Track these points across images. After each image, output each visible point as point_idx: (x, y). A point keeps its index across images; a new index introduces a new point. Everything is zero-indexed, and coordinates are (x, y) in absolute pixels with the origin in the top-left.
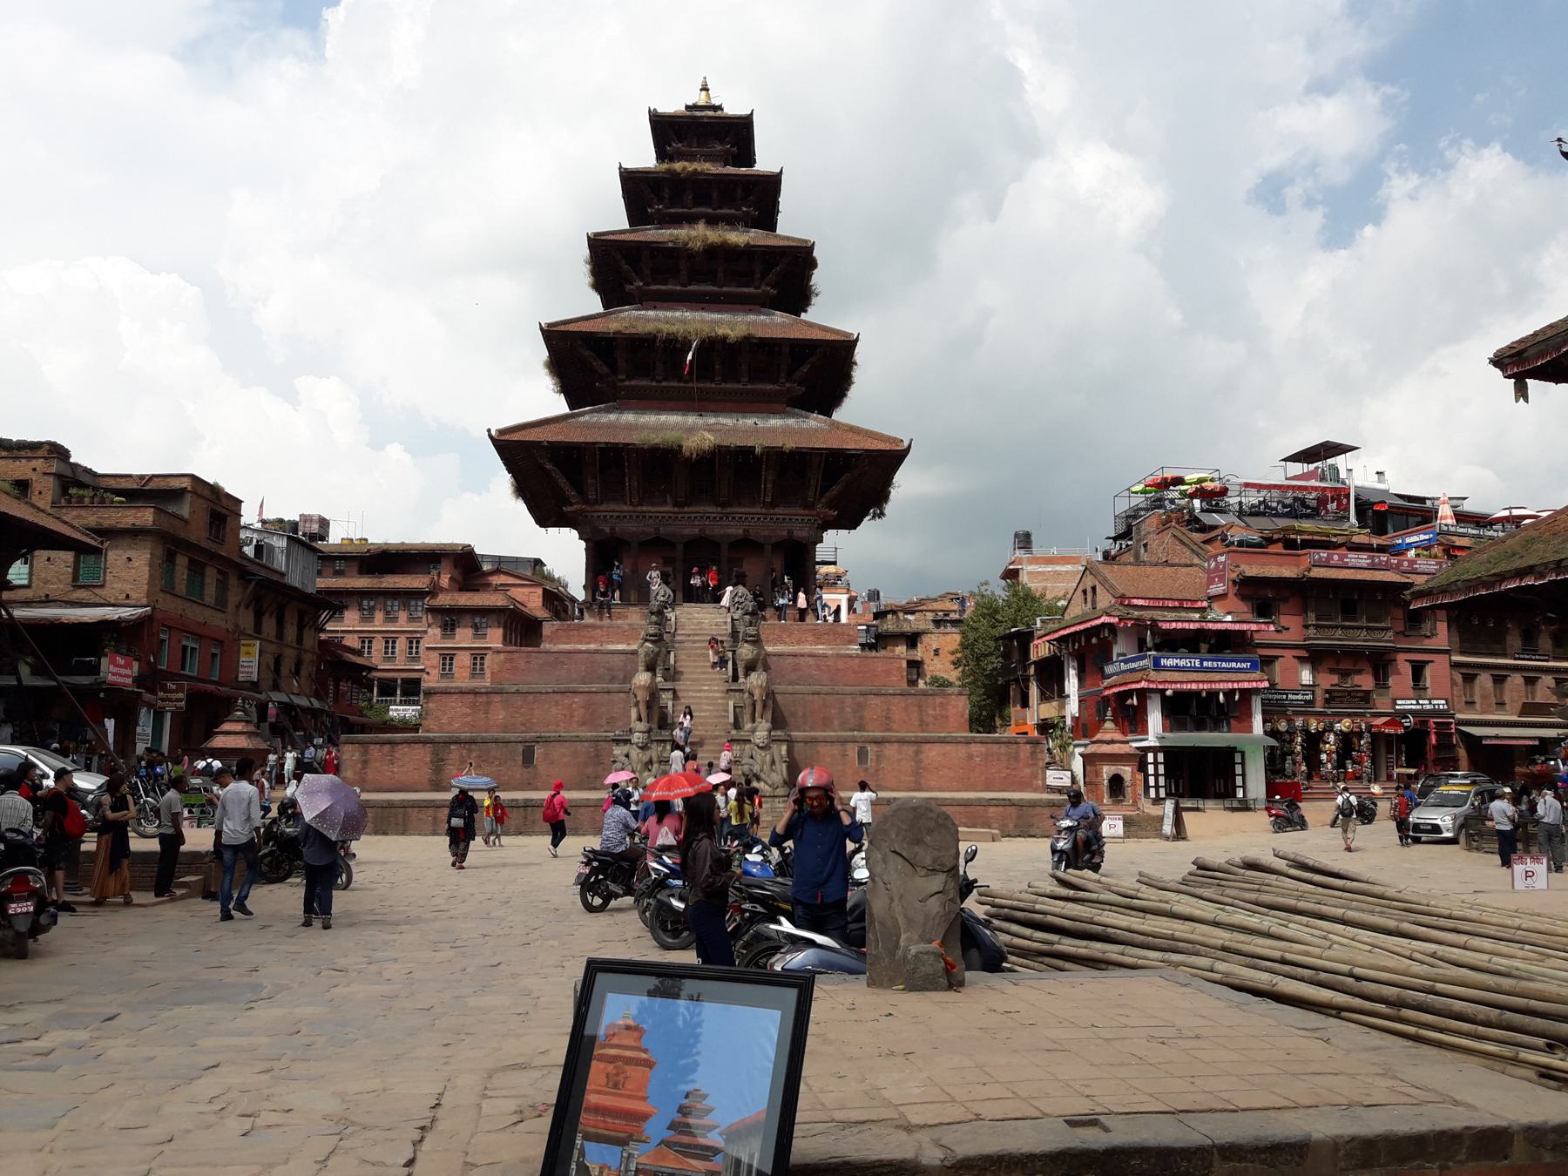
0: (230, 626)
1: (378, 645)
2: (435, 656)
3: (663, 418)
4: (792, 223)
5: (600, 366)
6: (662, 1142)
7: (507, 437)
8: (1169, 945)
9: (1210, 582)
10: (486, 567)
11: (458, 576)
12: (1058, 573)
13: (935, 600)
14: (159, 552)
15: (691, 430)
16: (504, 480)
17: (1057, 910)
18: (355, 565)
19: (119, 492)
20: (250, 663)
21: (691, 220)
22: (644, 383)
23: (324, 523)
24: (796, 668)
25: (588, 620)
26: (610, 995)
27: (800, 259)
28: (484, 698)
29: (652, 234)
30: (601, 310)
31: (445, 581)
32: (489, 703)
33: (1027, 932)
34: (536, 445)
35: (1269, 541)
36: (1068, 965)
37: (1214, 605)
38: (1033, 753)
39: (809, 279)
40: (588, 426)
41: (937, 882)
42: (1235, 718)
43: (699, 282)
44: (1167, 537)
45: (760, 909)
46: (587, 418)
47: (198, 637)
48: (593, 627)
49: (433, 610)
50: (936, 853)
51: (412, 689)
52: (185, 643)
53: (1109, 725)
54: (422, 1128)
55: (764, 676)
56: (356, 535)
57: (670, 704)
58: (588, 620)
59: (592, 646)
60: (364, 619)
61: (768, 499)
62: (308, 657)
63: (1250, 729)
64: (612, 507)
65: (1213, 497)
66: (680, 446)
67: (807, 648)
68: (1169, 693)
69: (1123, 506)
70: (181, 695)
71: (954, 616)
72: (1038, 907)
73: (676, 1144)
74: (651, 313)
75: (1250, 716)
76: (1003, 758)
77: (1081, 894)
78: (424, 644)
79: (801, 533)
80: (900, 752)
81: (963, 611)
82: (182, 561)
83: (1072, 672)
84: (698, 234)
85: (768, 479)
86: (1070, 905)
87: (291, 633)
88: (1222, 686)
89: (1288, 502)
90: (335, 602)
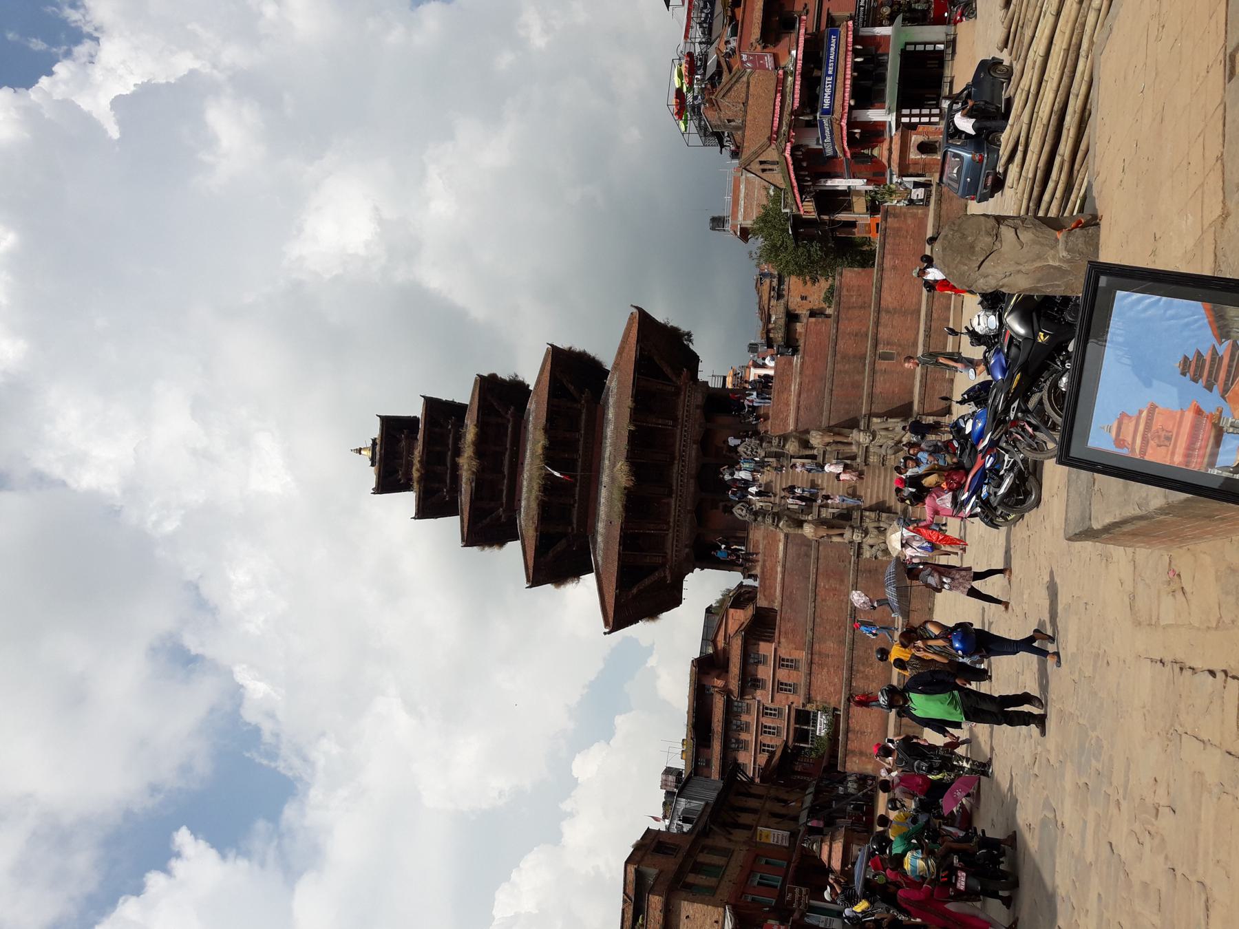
0: (745, 848)
1: (767, 739)
2: (778, 696)
3: (603, 500)
4: (461, 392)
5: (561, 545)
6: (1223, 397)
7: (611, 620)
8: (1074, 51)
9: (763, 67)
10: (710, 651)
12: (747, 195)
13: (761, 298)
14: (684, 894)
15: (613, 479)
17: (1035, 157)
19: (635, 919)
20: (775, 836)
21: (456, 467)
23: (668, 771)
25: (757, 571)
26: (1089, 445)
27: (489, 387)
28: (816, 658)
29: (465, 498)
30: (519, 542)
31: (719, 683)
32: (820, 654)
33: (1051, 185)
35: (733, 18)
36: (1083, 147)
37: (783, 64)
38: (895, 216)
39: (503, 381)
40: (606, 558)
41: (1007, 233)
42: (877, 49)
43: (502, 464)
44: (724, 102)
45: (1015, 405)
46: (599, 559)
47: (752, 872)
49: (742, 693)
50: (983, 233)
51: (804, 717)
52: (755, 883)
53: (876, 152)
54: (1181, 669)
55: (813, 433)
56: (679, 748)
57: (831, 510)
58: (757, 571)
59: (779, 569)
60: (746, 748)
61: (671, 423)
62: (773, 792)
63: (887, 38)
64: (669, 544)
65: (693, 64)
66: (625, 488)
67: (793, 398)
68: (852, 103)
69: (696, 139)
70: (797, 890)
71: (775, 283)
72: (1030, 175)
73: (1226, 384)
74: (523, 503)
75: (874, 37)
77: (1022, 140)
78: (768, 704)
79: (699, 399)
80: (886, 326)
81: (771, 275)
82: (691, 878)
83: (830, 183)
84: (467, 463)
86: (1031, 147)
87: (753, 803)
88: (849, 60)
89: (702, 5)
90: (731, 768)
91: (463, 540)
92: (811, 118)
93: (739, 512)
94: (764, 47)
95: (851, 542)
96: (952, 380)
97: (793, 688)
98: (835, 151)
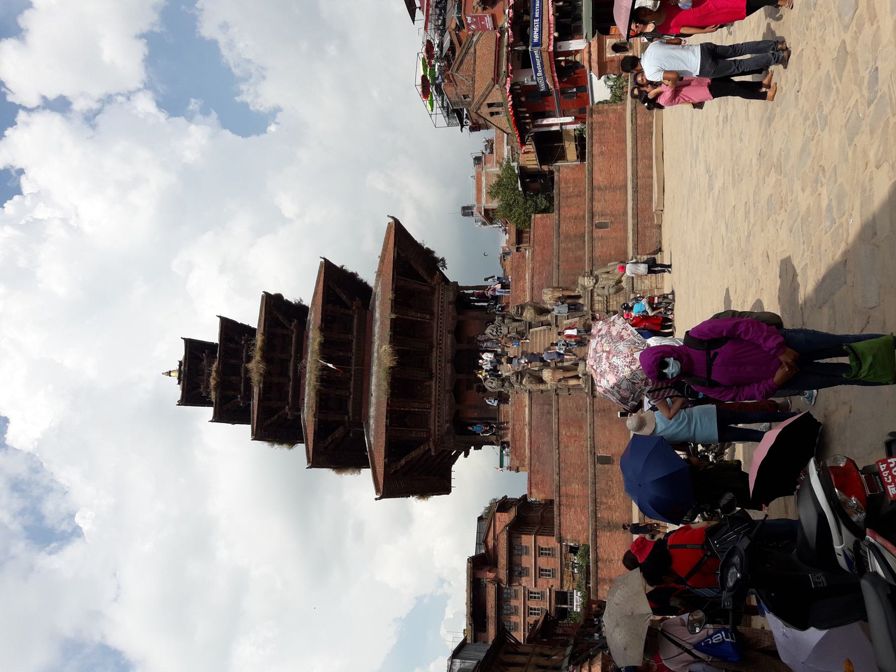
3: (373, 388)
5: (339, 433)
7: (381, 487)
9: (484, 28)
10: (483, 551)
11: (488, 568)
15: (380, 365)
16: (412, 500)
18: (479, 634)
22: (350, 404)
25: (508, 438)
28: (564, 500)
31: (491, 575)
32: (567, 495)
34: (387, 466)
38: (599, 113)
39: (288, 303)
44: (459, 76)
46: (372, 439)
48: (514, 429)
49: (510, 581)
51: (563, 597)
58: (508, 438)
59: (527, 431)
61: (428, 317)
62: (538, 650)
66: (391, 368)
67: (528, 285)
68: (556, 34)
76: (602, 132)
79: (451, 296)
80: (599, 201)
83: (546, 122)
85: (414, 315)
89: (438, 12)
91: (253, 434)
92: (524, 48)
94: (484, 9)
96: (660, 226)
97: (550, 573)
98: (547, 85)
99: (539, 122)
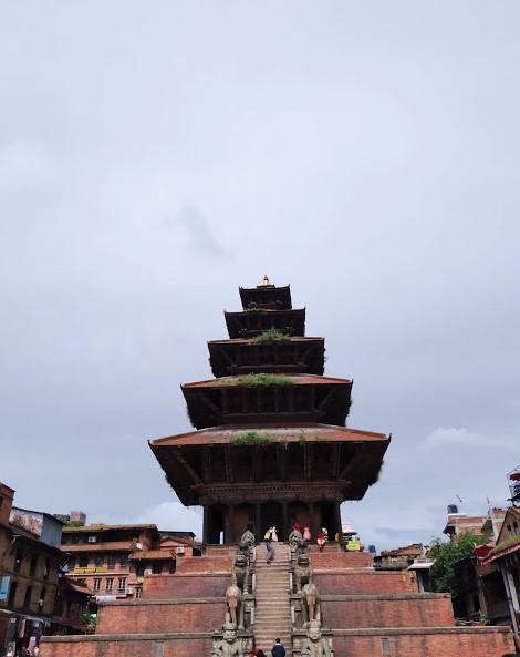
5: (213, 407)
11: (147, 540)
24: (334, 583)
27: (317, 347)
28: (134, 609)
29: (240, 341)
32: (138, 612)
38: (505, 640)
43: (267, 363)
48: (208, 560)
49: (133, 561)
55: (314, 587)
61: (309, 475)
62: (51, 588)
67: (341, 570)
76: (484, 644)
78: (127, 582)
83: (511, 582)
93: (248, 536)
95: (223, 629)
99: (510, 576)
